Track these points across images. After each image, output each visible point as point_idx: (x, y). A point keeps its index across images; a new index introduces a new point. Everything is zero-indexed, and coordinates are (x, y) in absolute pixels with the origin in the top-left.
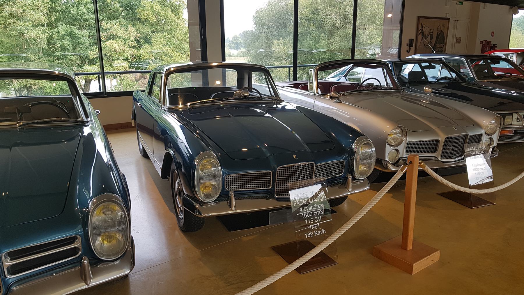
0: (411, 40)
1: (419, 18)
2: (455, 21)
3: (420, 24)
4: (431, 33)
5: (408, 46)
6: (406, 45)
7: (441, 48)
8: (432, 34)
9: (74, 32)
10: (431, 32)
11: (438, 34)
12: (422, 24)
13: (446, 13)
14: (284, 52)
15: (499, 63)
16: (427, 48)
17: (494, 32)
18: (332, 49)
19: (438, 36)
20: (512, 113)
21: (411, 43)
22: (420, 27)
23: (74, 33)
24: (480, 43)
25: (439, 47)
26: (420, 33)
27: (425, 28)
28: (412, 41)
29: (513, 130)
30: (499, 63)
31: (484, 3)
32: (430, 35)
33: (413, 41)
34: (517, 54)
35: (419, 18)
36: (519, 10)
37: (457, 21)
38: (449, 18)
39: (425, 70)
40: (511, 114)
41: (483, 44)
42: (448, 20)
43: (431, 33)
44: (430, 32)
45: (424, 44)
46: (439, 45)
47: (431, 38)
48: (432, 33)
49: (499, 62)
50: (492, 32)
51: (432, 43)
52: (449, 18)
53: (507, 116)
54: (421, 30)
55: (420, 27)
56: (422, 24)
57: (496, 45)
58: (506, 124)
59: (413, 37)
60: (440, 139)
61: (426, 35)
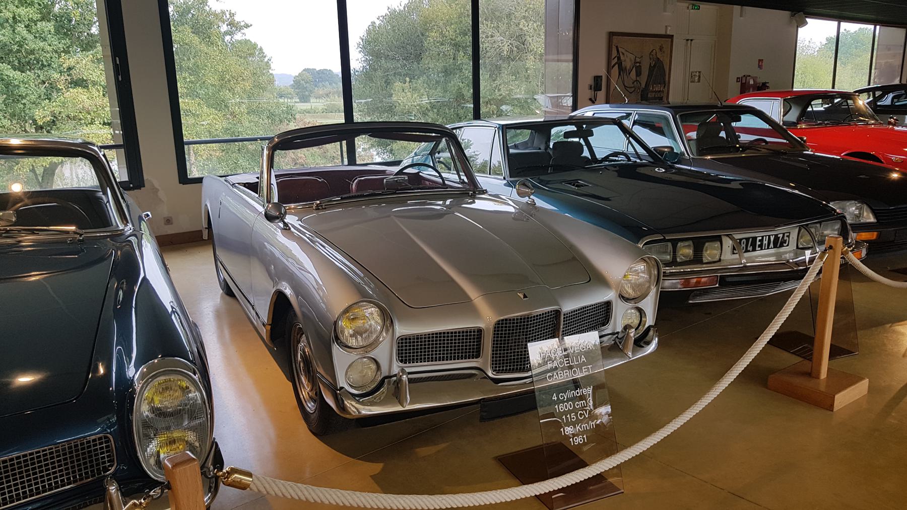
0: (597, 79)
1: (611, 35)
2: (687, 40)
3: (613, 46)
4: (638, 64)
5: (591, 89)
6: (587, 87)
7: (660, 91)
8: (640, 66)
9: (7, 75)
10: (637, 63)
11: (652, 66)
12: (617, 47)
13: (666, 26)
14: (413, 103)
15: (739, 120)
16: (631, 93)
17: (763, 60)
18: (499, 98)
19: (651, 69)
20: (720, 236)
21: (597, 84)
22: (614, 53)
23: (6, 77)
24: (737, 81)
25: (654, 90)
27: (623, 54)
28: (599, 80)
29: (717, 276)
30: (739, 120)
31: (740, 7)
32: (634, 68)
33: (602, 80)
34: (784, 100)
35: (611, 35)
36: (808, 20)
37: (692, 40)
38: (673, 36)
39: (589, 138)
40: (719, 239)
41: (743, 82)
42: (670, 39)
43: (638, 64)
44: (635, 63)
45: (625, 86)
46: (655, 85)
47: (639, 74)
48: (640, 63)
49: (740, 117)
50: (760, 60)
51: (640, 84)
52: (673, 36)
53: (707, 244)
54: (616, 58)
55: (614, 53)
56: (617, 47)
57: (767, 85)
58: (707, 261)
59: (602, 72)
60: (482, 325)
61: (628, 68)
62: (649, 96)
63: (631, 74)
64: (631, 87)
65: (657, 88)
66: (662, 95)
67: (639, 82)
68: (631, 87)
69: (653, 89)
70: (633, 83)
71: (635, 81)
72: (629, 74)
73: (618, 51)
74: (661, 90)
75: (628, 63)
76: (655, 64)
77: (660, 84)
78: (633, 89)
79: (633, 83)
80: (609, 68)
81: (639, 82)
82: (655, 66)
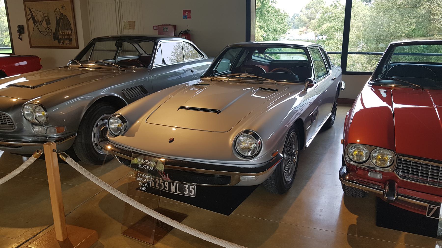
7: (68, 35)
10: (45, 17)
12: (29, 8)
16: (45, 35)
19: (58, 21)
22: (28, 12)
25: (63, 34)
26: (29, 19)
27: (34, 12)
32: (44, 21)
43: (47, 18)
44: (45, 17)
45: (39, 31)
46: (63, 31)
47: (48, 23)
50: (184, 11)
51: (51, 30)
54: (30, 15)
56: (29, 8)
59: (24, 23)
61: (40, 20)
62: (60, 37)
63: (42, 24)
64: (45, 32)
65: (66, 32)
66: (71, 37)
67: (50, 28)
70: (45, 29)
71: (47, 28)
73: (30, 11)
74: (69, 34)
75: (39, 16)
76: (60, 17)
77: (67, 30)
78: (46, 33)
79: (45, 29)
80: (28, 20)
81: (50, 28)
82: (60, 18)
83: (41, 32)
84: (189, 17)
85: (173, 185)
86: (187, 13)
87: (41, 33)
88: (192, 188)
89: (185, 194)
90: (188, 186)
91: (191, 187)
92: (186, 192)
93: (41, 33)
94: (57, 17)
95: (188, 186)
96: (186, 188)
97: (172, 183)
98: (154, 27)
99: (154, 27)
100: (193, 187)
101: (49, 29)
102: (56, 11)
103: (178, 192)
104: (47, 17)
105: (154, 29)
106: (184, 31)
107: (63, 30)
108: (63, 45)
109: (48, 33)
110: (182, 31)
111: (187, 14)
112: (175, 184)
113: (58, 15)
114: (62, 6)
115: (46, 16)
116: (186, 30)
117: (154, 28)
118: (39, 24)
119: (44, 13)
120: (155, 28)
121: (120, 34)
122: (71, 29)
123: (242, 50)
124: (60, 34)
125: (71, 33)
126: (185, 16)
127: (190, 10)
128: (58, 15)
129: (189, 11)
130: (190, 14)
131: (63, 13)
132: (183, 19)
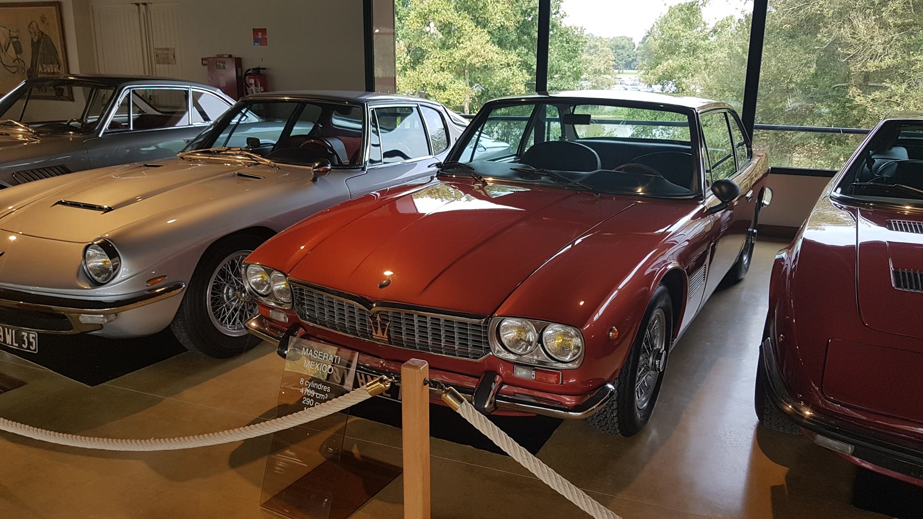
7: (53, 73)
16: (14, 73)
19: (35, 46)
32: (11, 45)
43: (15, 40)
45: (3, 64)
46: (44, 65)
47: (18, 50)
48: (17, 38)
50: (256, 31)
51: (23, 62)
63: (8, 51)
64: (14, 67)
65: (50, 69)
68: (14, 67)
69: (43, 70)
70: (14, 62)
72: (6, 51)
77: (52, 64)
78: (15, 69)
79: (14, 62)
82: (39, 41)
83: (7, 67)
84: (263, 42)
85: (8, 333)
86: (260, 34)
87: (6, 68)
88: (33, 338)
89: (23, 348)
90: (26, 334)
91: (31, 335)
92: (33, 346)
93: (6, 68)
94: (34, 39)
95: (26, 334)
96: (25, 338)
97: (6, 329)
98: (203, 59)
99: (203, 59)
100: (34, 336)
101: (20, 61)
102: (32, 26)
103: (14, 344)
104: (15, 37)
105: (203, 64)
106: (253, 69)
107: (44, 64)
108: (46, 92)
109: (19, 68)
110: (249, 70)
111: (260, 37)
112: (10, 330)
113: (35, 34)
114: (40, 18)
115: (14, 36)
116: (257, 67)
117: (203, 62)
118: (3, 51)
119: (10, 31)
120: (205, 62)
121: (145, 73)
122: (58, 63)
123: (298, 106)
124: (39, 71)
125: (59, 70)
126: (256, 40)
127: (265, 29)
128: (35, 34)
129: (264, 31)
130: (265, 36)
131: (44, 32)
132: (254, 45)
